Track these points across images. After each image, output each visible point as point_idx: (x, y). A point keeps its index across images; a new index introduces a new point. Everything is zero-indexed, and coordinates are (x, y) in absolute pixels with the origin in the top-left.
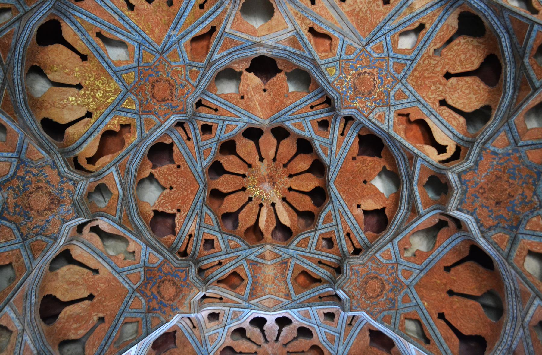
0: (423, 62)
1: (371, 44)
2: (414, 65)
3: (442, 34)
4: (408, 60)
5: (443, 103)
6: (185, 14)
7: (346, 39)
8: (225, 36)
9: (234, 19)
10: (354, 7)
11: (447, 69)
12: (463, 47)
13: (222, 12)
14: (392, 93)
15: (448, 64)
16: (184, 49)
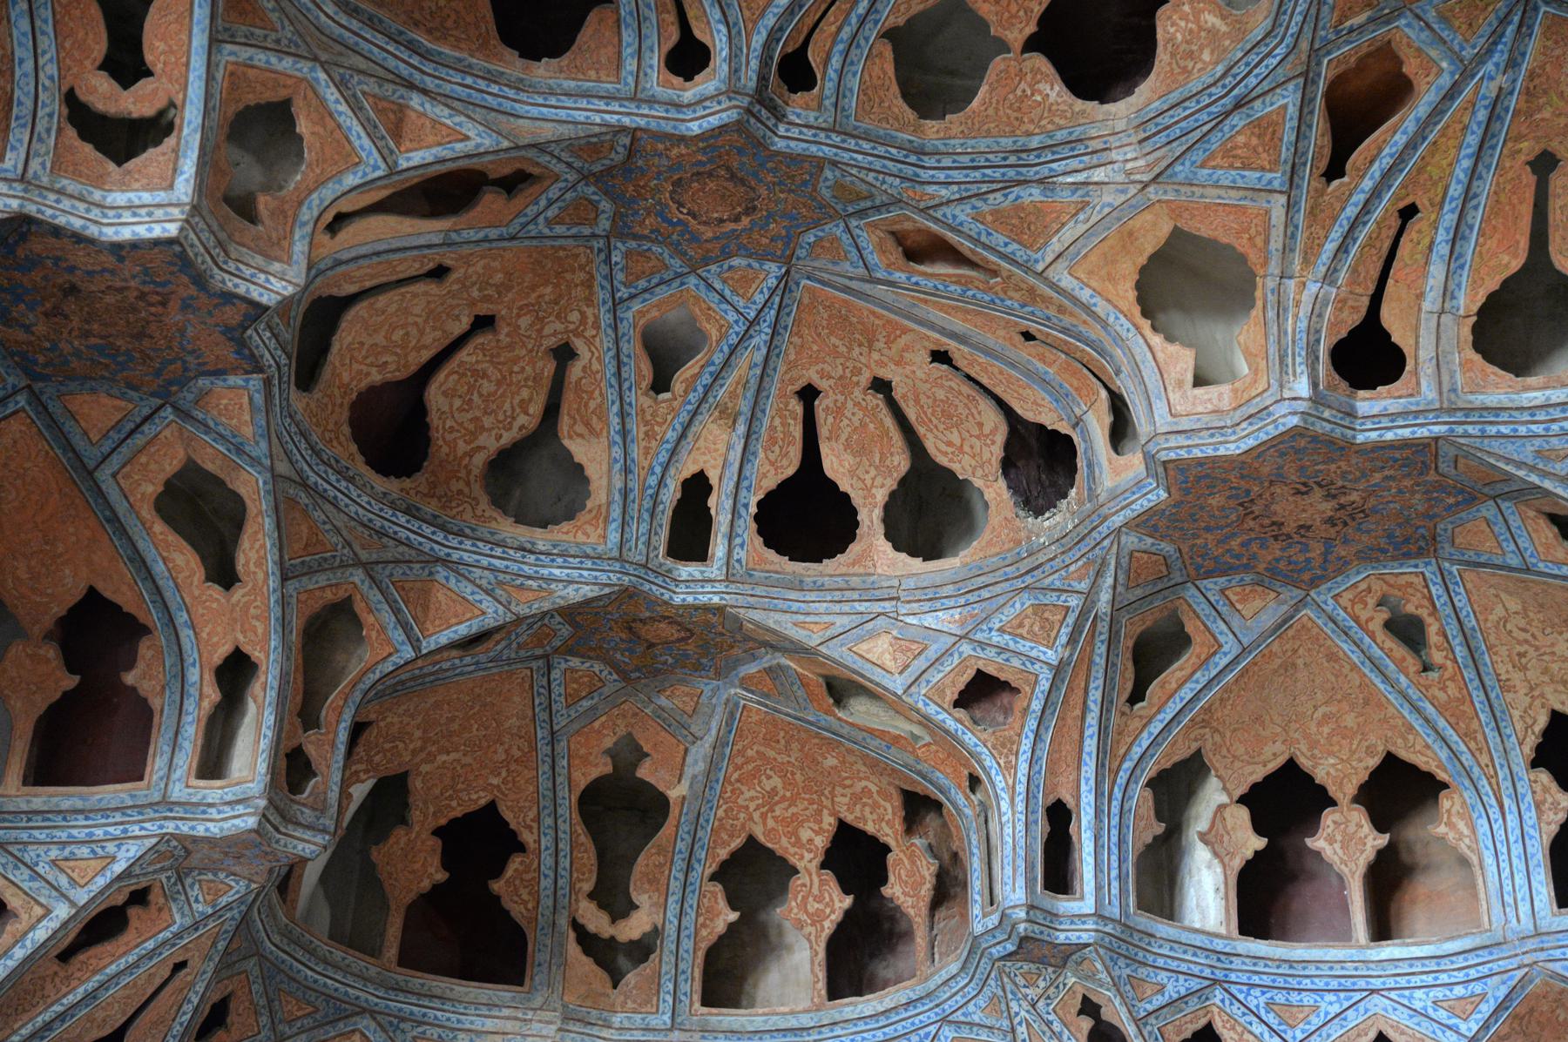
0: (583, 314)
1: (772, 282)
2: (602, 295)
3: (592, 405)
4: (632, 297)
5: (439, 273)
6: (1467, 163)
7: (862, 271)
8: (1277, 178)
9: (1267, 241)
10: (895, 348)
11: (502, 337)
12: (507, 406)
13: (1321, 246)
14: (605, 205)
15: (511, 347)
16: (1433, 53)
